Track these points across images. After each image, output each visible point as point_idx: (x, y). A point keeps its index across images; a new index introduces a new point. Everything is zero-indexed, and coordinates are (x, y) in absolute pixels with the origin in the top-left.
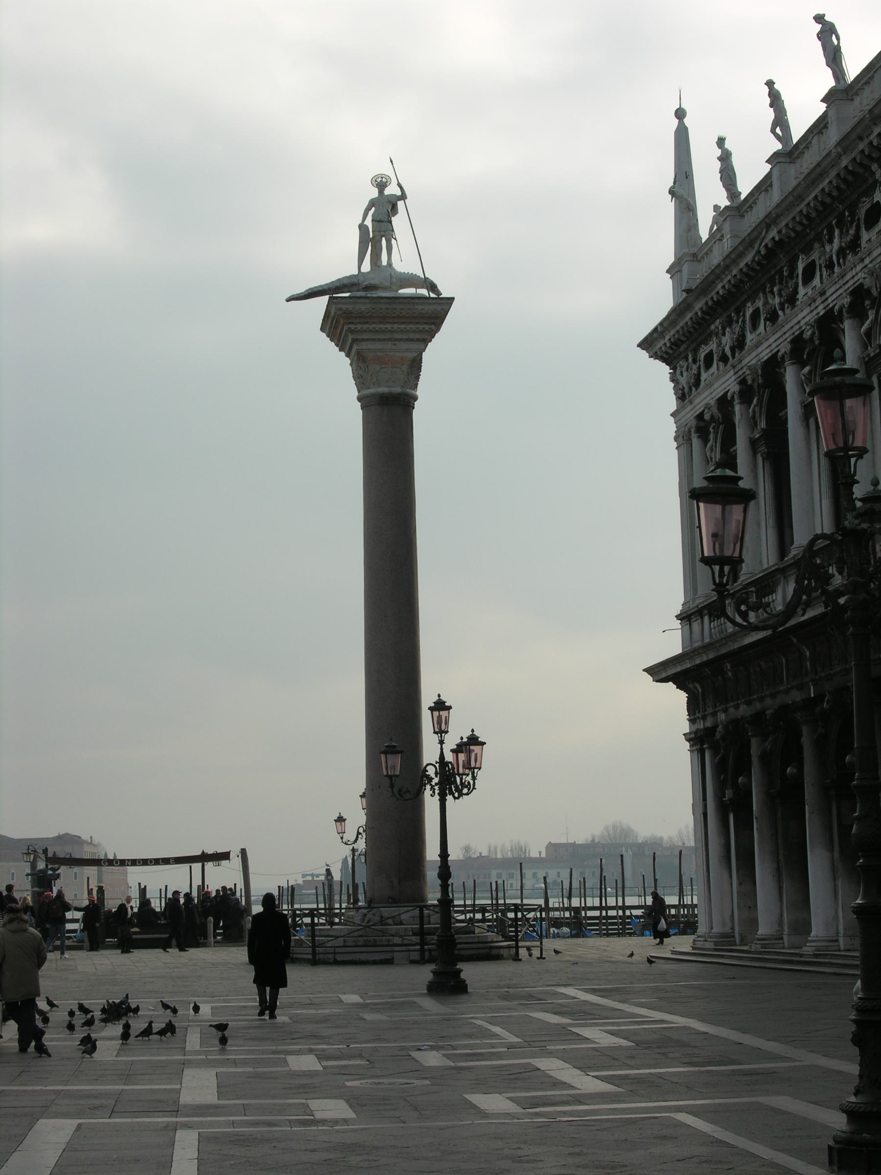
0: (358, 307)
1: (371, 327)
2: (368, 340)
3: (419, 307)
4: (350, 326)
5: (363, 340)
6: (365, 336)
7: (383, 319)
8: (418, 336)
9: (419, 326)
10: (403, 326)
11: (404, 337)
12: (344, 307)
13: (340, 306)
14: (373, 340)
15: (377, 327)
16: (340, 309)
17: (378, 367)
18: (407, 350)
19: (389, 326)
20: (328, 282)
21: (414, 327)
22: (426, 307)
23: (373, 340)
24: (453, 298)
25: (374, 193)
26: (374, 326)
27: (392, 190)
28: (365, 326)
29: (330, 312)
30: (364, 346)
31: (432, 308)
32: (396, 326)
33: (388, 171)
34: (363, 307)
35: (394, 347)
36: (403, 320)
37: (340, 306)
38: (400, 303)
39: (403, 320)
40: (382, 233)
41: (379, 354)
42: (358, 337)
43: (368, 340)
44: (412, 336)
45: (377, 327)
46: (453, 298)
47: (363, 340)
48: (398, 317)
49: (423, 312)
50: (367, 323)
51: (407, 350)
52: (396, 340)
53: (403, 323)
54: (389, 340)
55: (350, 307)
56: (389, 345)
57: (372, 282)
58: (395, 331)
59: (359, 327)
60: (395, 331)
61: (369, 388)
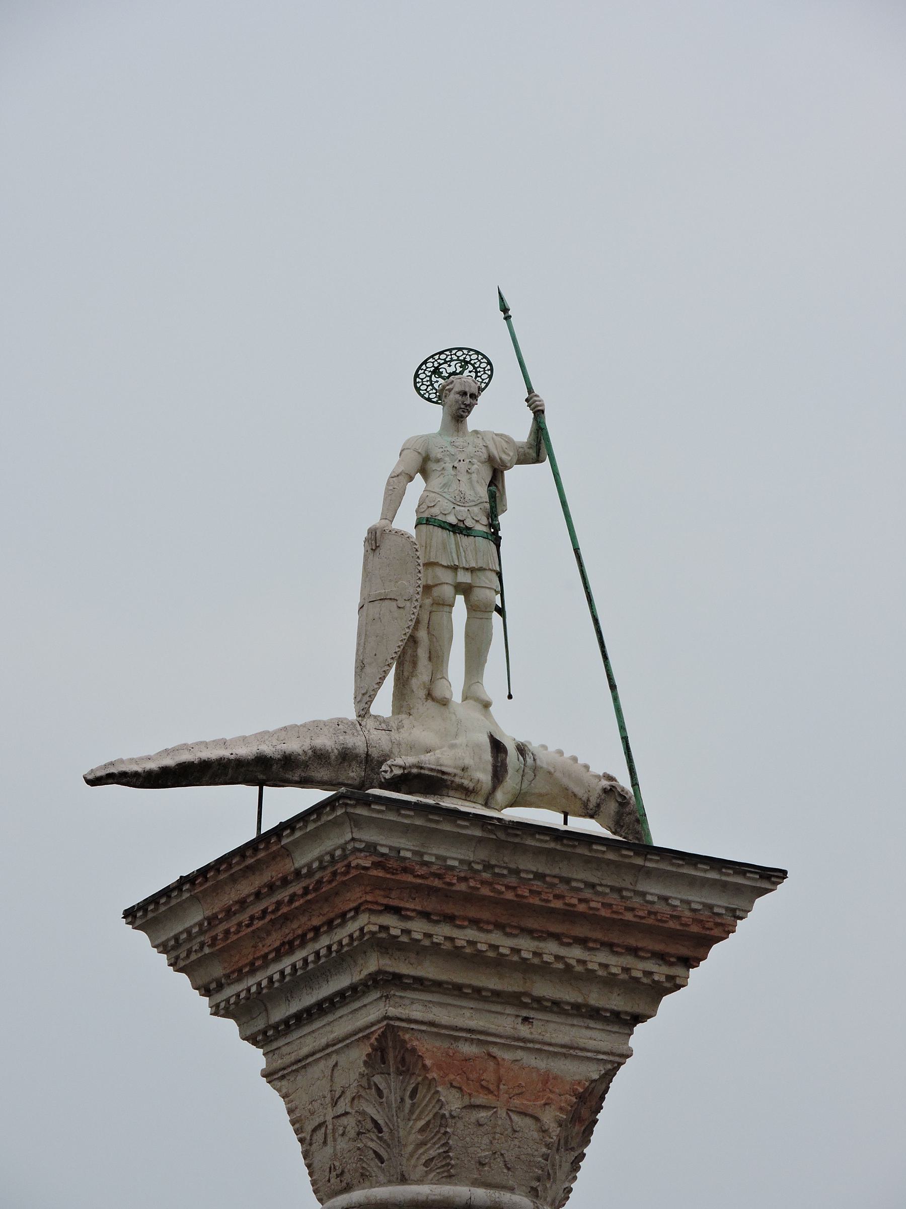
0: (435, 851)
1: (464, 936)
2: (437, 986)
3: (654, 889)
4: (388, 920)
5: (420, 984)
6: (429, 970)
7: (512, 914)
8: (616, 1002)
9: (628, 961)
10: (575, 953)
11: (568, 995)
12: (385, 841)
13: (369, 835)
14: (457, 990)
15: (484, 940)
16: (371, 848)
17: (453, 1102)
18: (569, 1051)
19: (527, 946)
20: (273, 726)
21: (616, 963)
22: (677, 894)
23: (457, 990)
24: (781, 874)
25: (431, 418)
26: (471, 934)
28: (442, 931)
29: (287, 852)
31: (698, 898)
32: (551, 948)
33: (492, 341)
34: (455, 855)
35: (524, 1031)
36: (580, 931)
37: (369, 835)
38: (588, 861)
39: (580, 931)
40: (464, 578)
41: (467, 1049)
42: (404, 969)
43: (437, 986)
44: (596, 998)
45: (484, 940)
46: (781, 874)
47: (420, 984)
48: (569, 915)
49: (660, 907)
50: (450, 919)
51: (569, 1051)
52: (539, 1003)
54: (514, 999)
55: (407, 845)
56: (504, 1023)
57: (429, 760)
58: (544, 970)
59: (418, 928)
60: (544, 970)
61: (403, 1180)
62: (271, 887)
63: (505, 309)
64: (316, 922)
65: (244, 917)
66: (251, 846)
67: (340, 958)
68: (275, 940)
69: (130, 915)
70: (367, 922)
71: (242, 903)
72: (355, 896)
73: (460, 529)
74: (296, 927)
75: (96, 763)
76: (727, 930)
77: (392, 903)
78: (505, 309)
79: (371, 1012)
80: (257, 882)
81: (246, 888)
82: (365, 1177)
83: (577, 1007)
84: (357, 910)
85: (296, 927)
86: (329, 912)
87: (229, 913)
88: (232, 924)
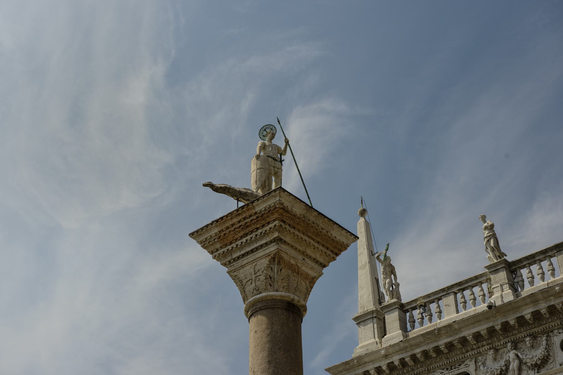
27: (279, 142)
30: (284, 247)
53: (318, 243)
61: (277, 291)
62: (245, 219)
63: (279, 121)
64: (258, 226)
65: (233, 228)
66: (237, 210)
67: (266, 234)
68: (241, 234)
69: (191, 235)
70: (276, 223)
71: (233, 225)
72: (276, 215)
73: (274, 159)
74: (250, 229)
75: (206, 181)
76: (346, 249)
77: (284, 220)
78: (279, 121)
79: (273, 248)
80: (240, 218)
81: (235, 220)
82: (266, 290)
83: (314, 259)
84: (274, 221)
85: (250, 229)
86: (263, 222)
87: (227, 228)
88: (227, 231)
